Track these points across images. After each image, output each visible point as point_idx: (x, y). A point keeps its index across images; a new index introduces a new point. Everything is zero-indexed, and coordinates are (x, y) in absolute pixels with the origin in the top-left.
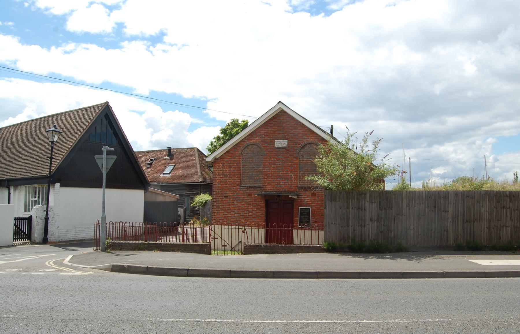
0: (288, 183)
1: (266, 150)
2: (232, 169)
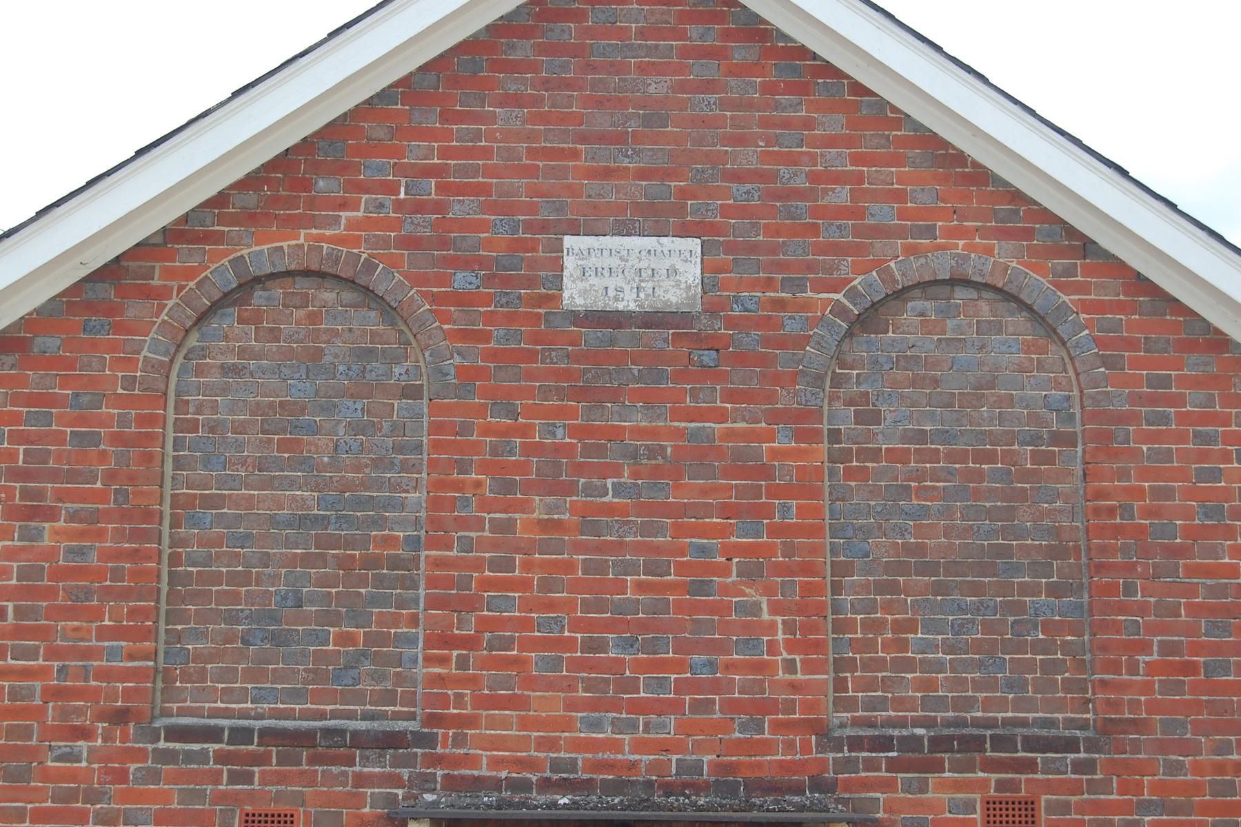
0: (716, 686)
1: (465, 335)
2: (57, 532)
